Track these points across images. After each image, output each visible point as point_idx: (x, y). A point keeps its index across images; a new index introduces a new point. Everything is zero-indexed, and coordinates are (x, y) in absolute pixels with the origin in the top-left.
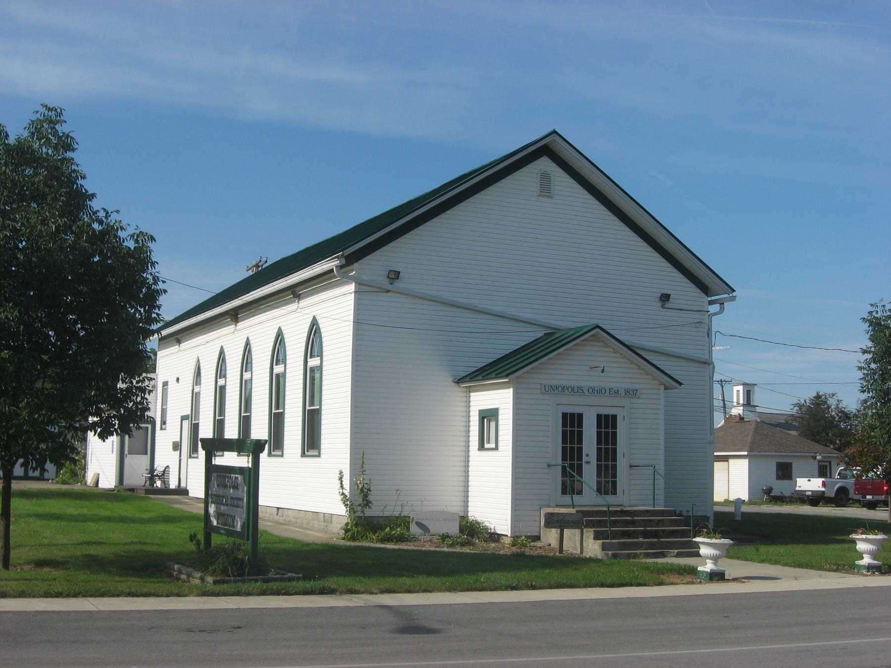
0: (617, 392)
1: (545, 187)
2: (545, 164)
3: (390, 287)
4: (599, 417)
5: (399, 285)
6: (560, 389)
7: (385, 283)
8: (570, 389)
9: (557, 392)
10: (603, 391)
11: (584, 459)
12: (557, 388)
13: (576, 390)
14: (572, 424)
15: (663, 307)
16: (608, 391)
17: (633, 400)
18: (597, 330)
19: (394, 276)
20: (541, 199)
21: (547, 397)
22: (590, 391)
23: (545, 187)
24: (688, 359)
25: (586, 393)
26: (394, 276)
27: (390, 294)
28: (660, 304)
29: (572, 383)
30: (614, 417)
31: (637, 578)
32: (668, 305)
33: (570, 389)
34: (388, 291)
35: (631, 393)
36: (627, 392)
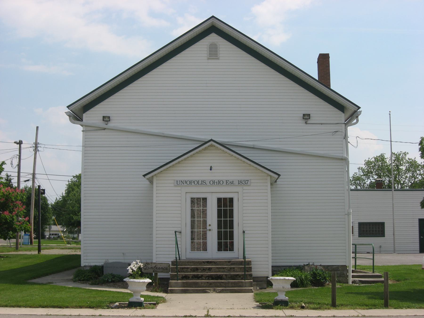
0: (232, 183)
1: (213, 53)
2: (213, 38)
3: (105, 126)
4: (219, 200)
5: (111, 125)
6: (188, 183)
7: (102, 124)
8: (196, 183)
9: (185, 184)
10: (221, 182)
11: (208, 228)
12: (186, 182)
13: (200, 182)
14: (198, 204)
15: (306, 123)
16: (225, 183)
17: (245, 188)
18: (212, 143)
19: (106, 119)
20: (210, 61)
21: (179, 188)
22: (211, 183)
23: (213, 53)
24: (329, 158)
25: (208, 184)
26: (106, 119)
27: (105, 131)
28: (304, 121)
29: (224, 178)
30: (231, 200)
31: (9, 303)
32: (309, 122)
33: (196, 183)
34: (104, 129)
35: (243, 183)
36: (240, 182)
